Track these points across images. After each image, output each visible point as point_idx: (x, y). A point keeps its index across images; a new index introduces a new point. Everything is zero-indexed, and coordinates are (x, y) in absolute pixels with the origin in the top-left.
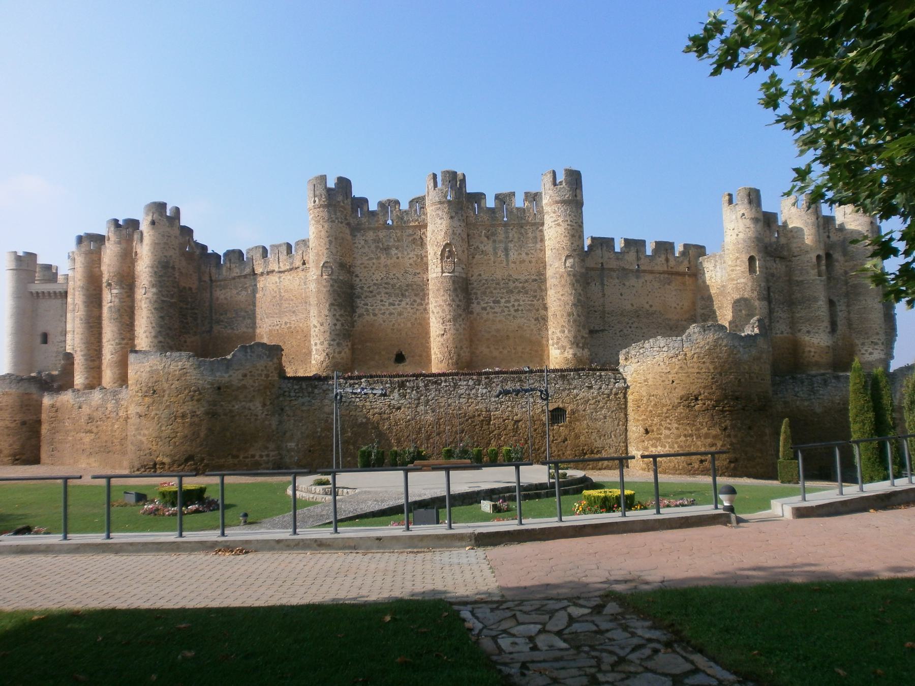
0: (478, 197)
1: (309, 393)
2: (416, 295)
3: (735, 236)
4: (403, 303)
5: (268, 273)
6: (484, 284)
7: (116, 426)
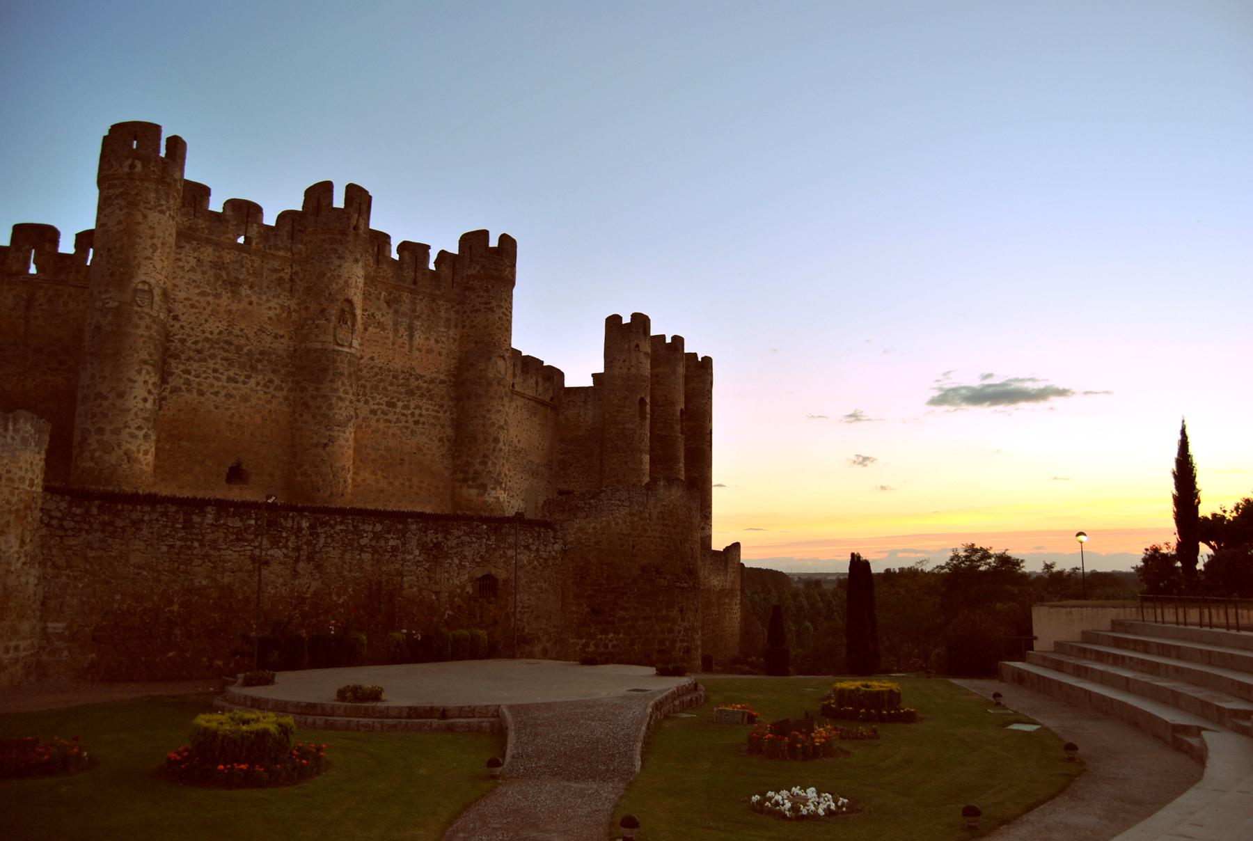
1: (104, 524)
2: (274, 372)
3: (625, 371)
4: (253, 381)
6: (377, 374)
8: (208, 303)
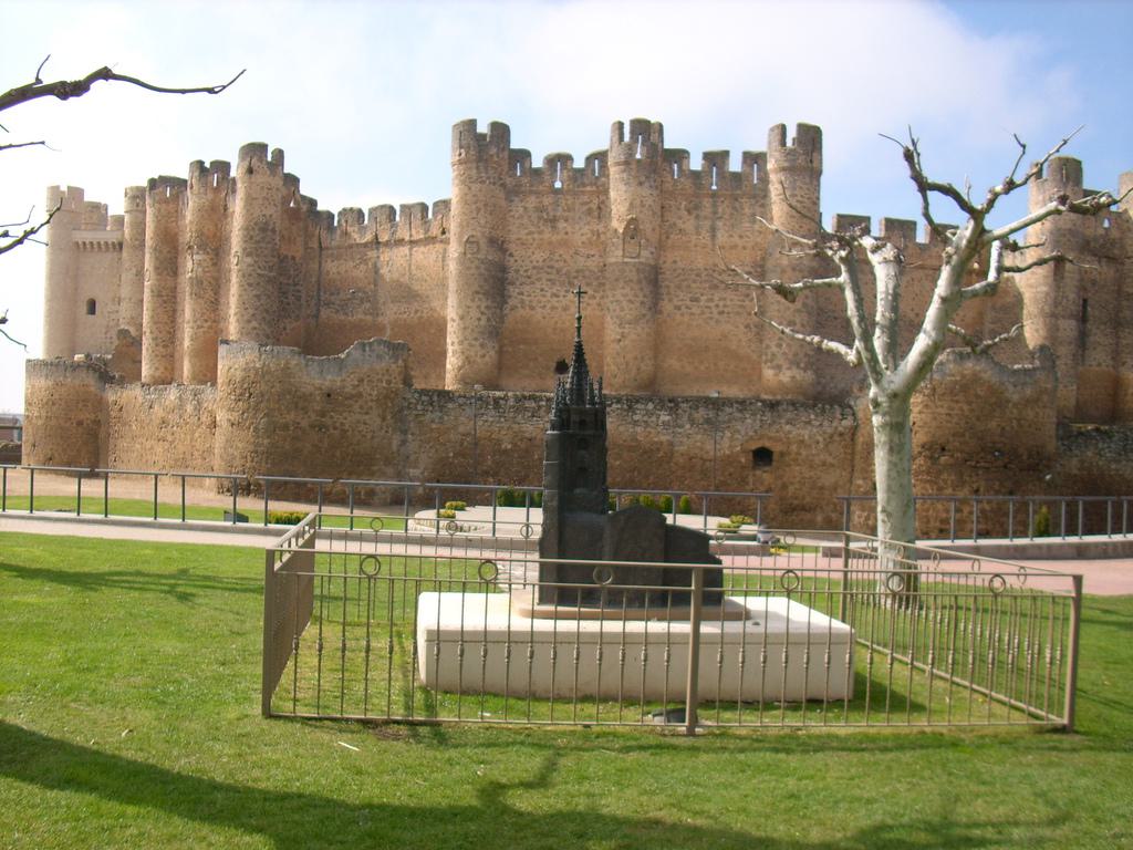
0: (680, 155)
7: (197, 435)
8: (534, 240)
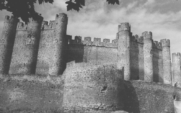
5: (93, 46)
